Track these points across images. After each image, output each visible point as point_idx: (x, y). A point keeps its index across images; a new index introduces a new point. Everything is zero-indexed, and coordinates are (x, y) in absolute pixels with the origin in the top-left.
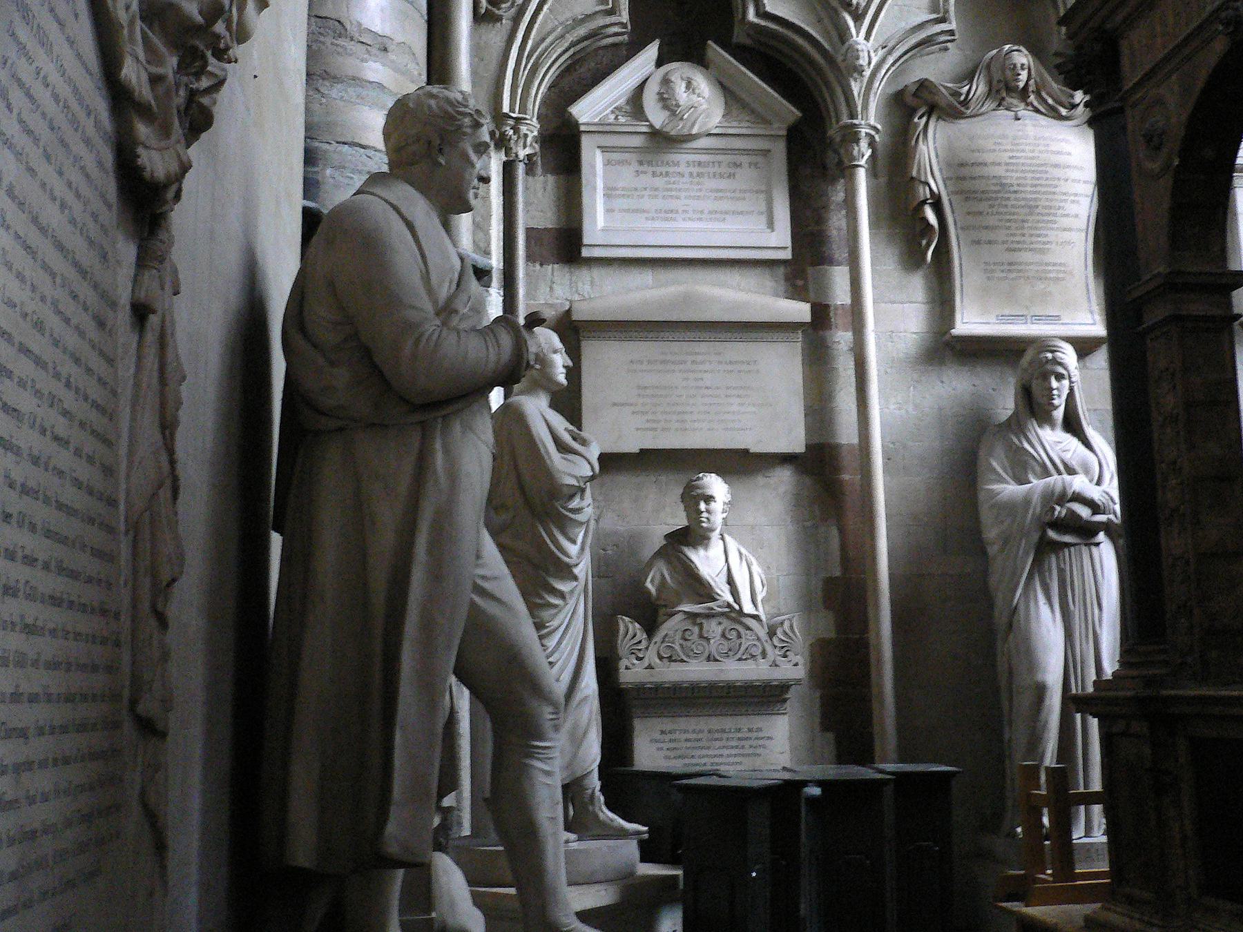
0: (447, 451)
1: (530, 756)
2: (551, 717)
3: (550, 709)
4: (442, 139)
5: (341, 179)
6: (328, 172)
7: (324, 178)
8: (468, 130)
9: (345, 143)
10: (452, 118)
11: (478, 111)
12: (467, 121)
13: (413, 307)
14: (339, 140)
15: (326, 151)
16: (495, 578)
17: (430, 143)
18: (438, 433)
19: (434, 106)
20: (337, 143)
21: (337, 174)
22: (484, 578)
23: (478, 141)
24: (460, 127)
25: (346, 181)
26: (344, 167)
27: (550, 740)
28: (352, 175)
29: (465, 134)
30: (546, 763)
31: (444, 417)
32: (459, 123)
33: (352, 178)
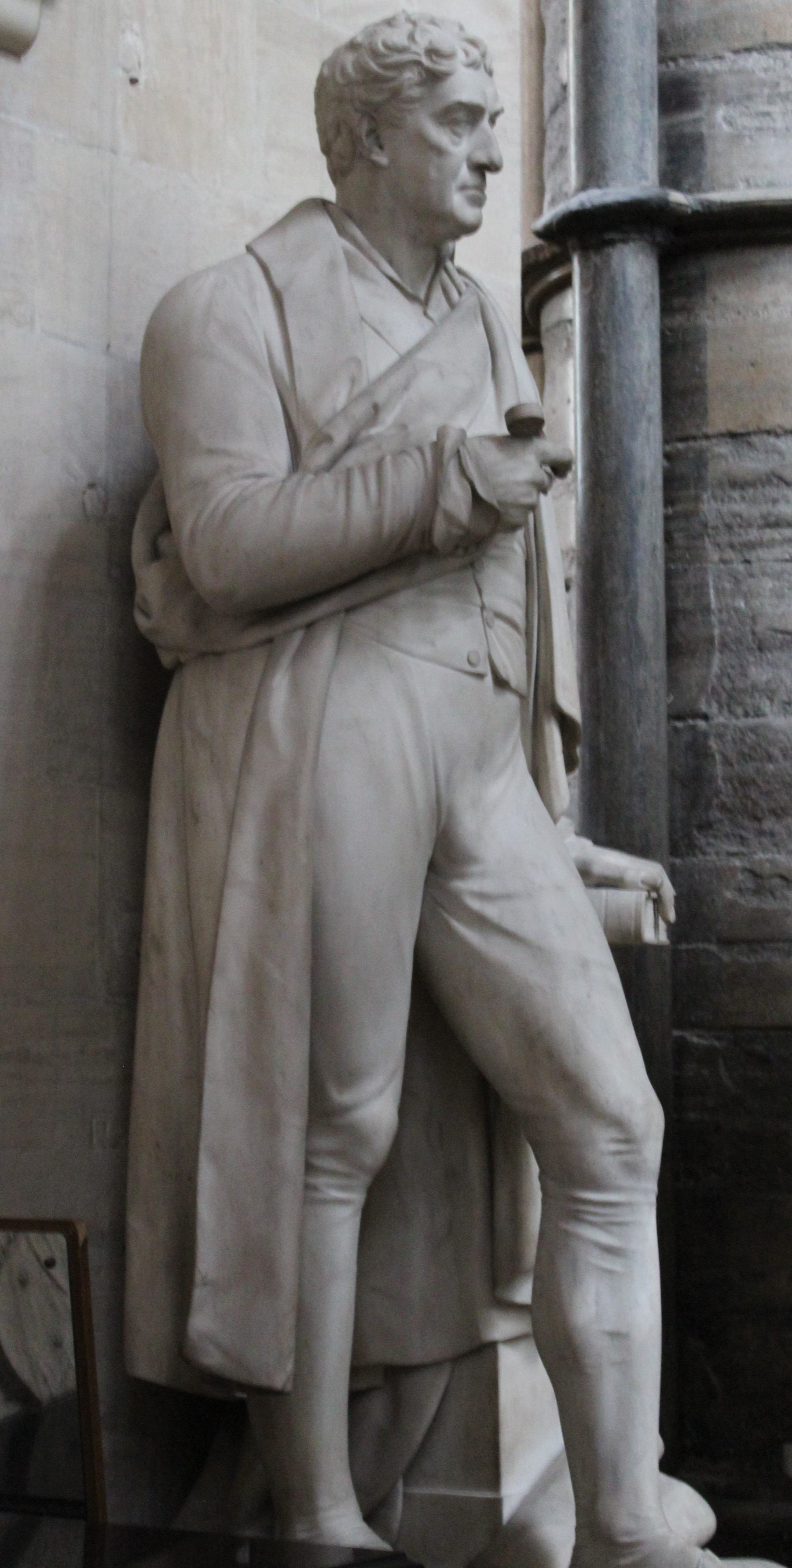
0: (296, 687)
1: (576, 1217)
2: (613, 1147)
3: (614, 1133)
4: (372, 119)
5: (746, 122)
6: (720, 113)
7: (712, 126)
8: (415, 92)
9: (748, 50)
10: (376, 79)
11: (432, 52)
12: (410, 76)
13: (211, 452)
14: (737, 45)
15: (713, 76)
16: (508, 897)
17: (351, 132)
18: (285, 661)
19: (350, 69)
20: (736, 52)
21: (734, 112)
22: (483, 896)
23: (439, 105)
24: (396, 93)
25: (755, 123)
26: (749, 97)
27: (618, 1189)
28: (766, 108)
29: (412, 100)
30: (608, 1231)
31: (310, 626)
32: (391, 85)
33: (768, 114)
